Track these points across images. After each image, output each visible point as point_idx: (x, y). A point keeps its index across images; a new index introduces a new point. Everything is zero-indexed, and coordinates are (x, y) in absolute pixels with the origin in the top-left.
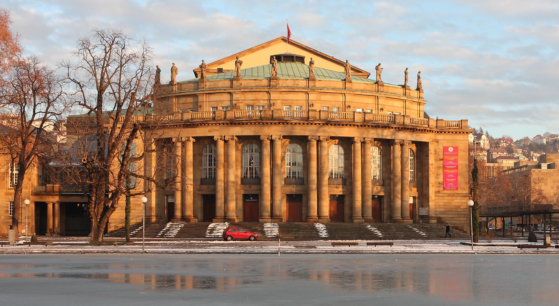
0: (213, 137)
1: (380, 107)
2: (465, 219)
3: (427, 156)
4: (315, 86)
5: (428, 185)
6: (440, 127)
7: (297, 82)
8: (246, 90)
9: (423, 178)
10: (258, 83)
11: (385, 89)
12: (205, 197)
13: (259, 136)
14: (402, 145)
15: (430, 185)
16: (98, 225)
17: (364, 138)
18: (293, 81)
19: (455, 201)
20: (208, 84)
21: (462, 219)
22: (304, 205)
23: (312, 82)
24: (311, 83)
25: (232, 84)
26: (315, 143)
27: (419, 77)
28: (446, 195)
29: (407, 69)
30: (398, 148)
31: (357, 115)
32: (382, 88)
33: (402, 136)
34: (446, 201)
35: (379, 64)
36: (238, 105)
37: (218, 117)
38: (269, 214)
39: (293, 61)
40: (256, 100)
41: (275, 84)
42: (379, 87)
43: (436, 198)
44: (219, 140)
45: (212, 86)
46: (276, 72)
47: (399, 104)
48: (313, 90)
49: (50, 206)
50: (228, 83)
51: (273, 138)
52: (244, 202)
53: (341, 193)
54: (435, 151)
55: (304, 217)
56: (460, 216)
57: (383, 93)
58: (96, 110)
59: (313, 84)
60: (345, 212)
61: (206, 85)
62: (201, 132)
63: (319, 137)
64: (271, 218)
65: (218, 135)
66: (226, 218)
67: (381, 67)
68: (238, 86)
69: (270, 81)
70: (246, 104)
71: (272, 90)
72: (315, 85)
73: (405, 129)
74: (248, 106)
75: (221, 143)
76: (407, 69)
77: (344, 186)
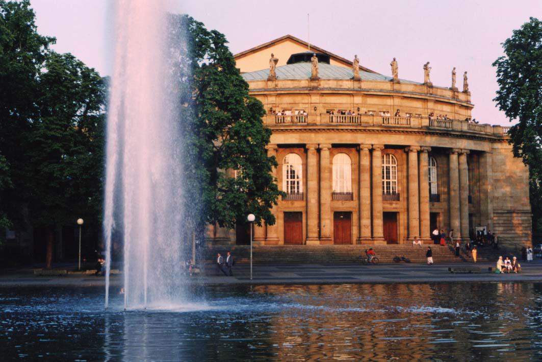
7: (340, 83)
10: (296, 84)
14: (460, 155)
18: (335, 82)
26: (368, 152)
28: (506, 212)
29: (454, 69)
30: (454, 158)
32: (431, 90)
34: (505, 218)
35: (428, 63)
38: (316, 235)
40: (295, 104)
43: (495, 215)
52: (285, 221)
57: (433, 96)
59: (359, 85)
60: (399, 230)
64: (319, 240)
66: (267, 240)
67: (429, 66)
72: (361, 86)
76: (454, 69)
77: (398, 202)
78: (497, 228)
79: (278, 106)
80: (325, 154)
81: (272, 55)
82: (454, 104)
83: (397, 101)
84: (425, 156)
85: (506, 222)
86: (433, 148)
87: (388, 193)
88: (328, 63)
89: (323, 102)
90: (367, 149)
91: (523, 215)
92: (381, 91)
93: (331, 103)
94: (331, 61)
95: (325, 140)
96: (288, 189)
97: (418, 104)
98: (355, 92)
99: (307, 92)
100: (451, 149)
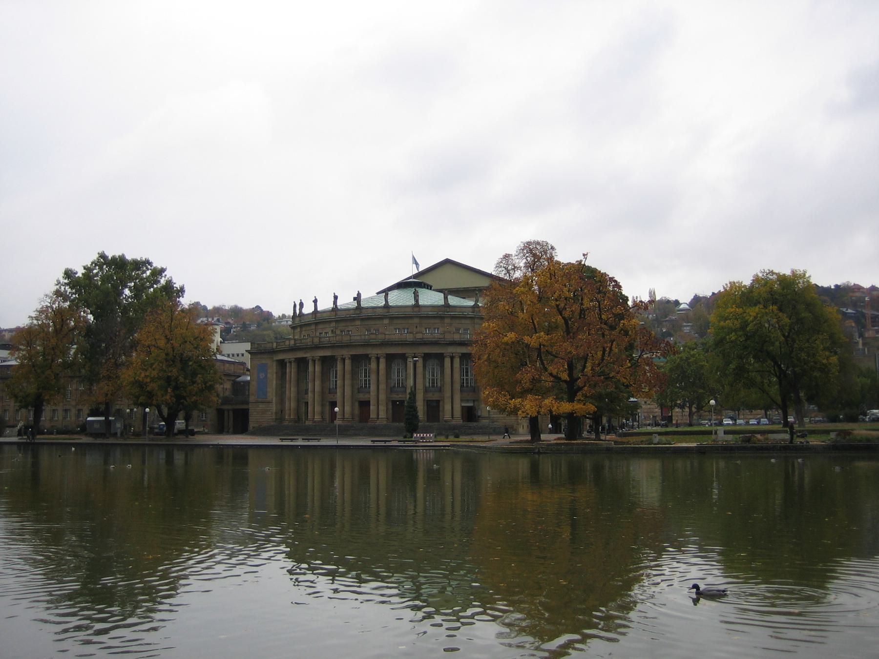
0: (306, 357)
4: (389, 311)
7: (375, 310)
13: (334, 356)
33: (450, 350)
49: (226, 413)
57: (450, 313)
80: (348, 362)
81: (334, 294)
83: (416, 321)
87: (467, 386)
89: (364, 324)
95: (346, 353)
96: (429, 384)
97: (437, 321)
100: (443, 354)
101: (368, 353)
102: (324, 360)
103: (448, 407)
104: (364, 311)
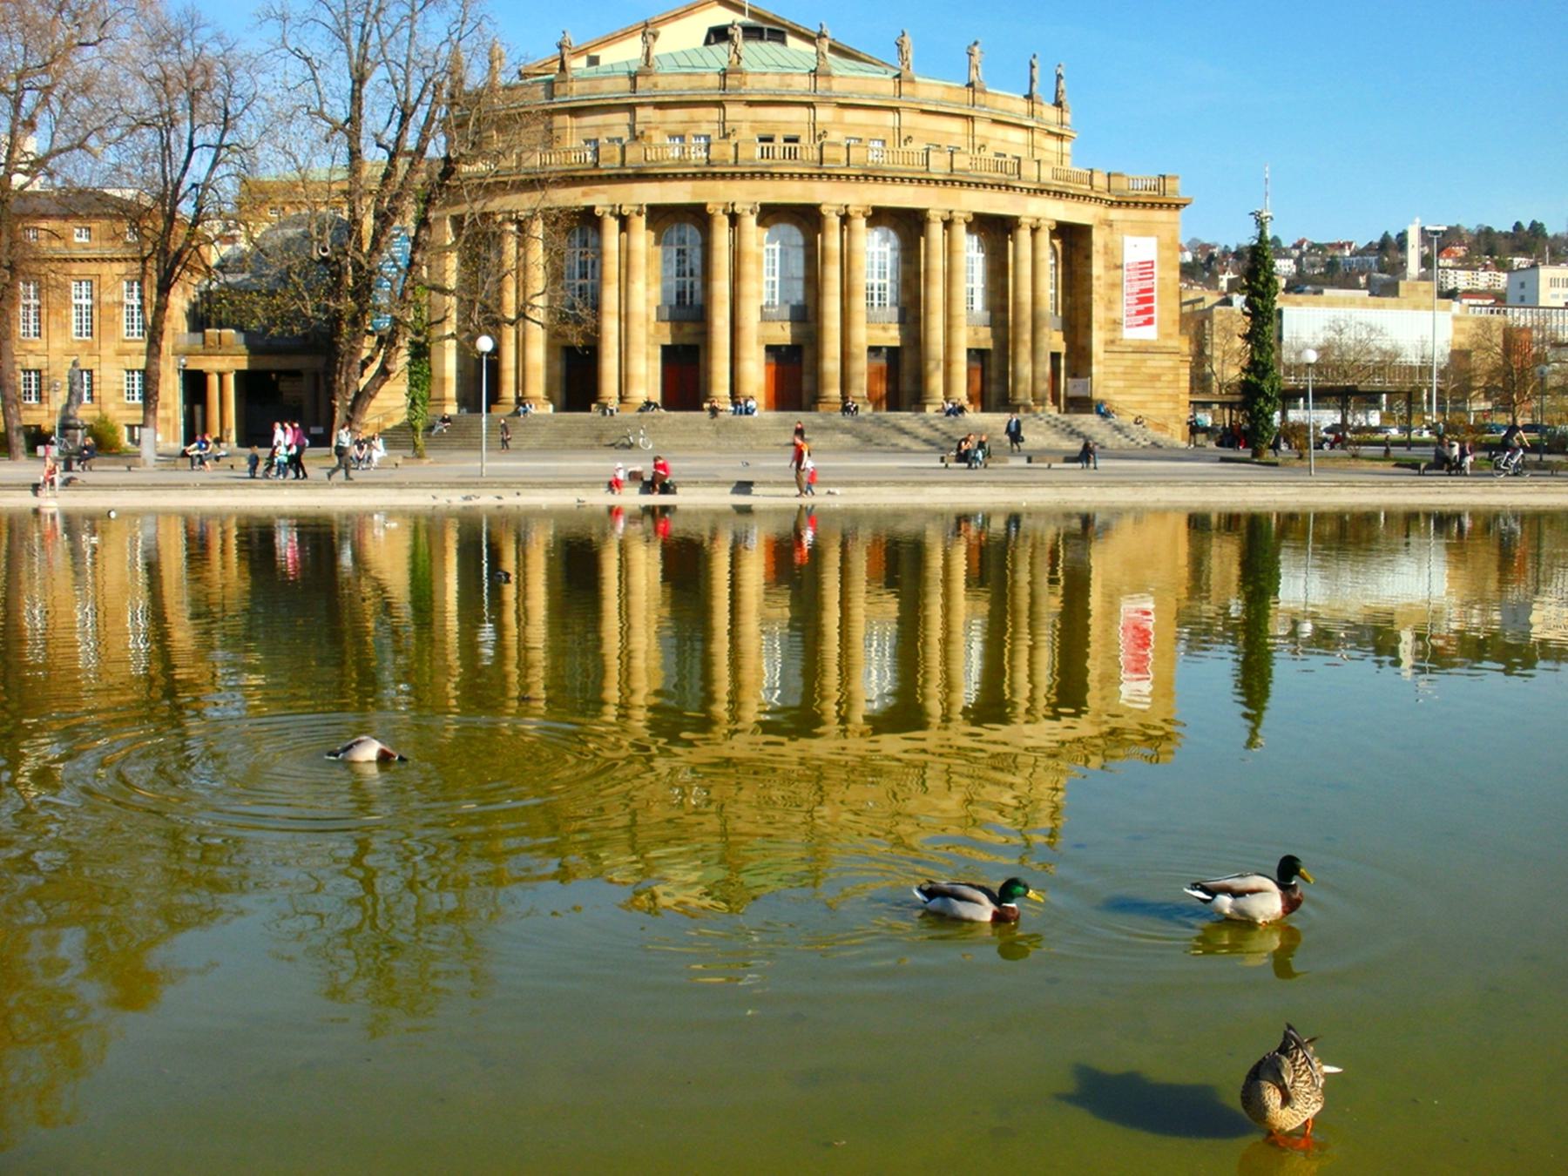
0: (593, 208)
1: (978, 142)
2: (1171, 405)
3: (1088, 257)
4: (829, 89)
5: (1089, 326)
6: (1116, 190)
7: (788, 79)
8: (667, 99)
9: (1076, 309)
10: (696, 82)
11: (988, 100)
12: (569, 351)
15: (1095, 326)
16: (348, 417)
17: (951, 212)
18: (777, 78)
19: (1150, 363)
20: (576, 86)
21: (1164, 405)
22: (805, 369)
23: (824, 79)
24: (821, 83)
25: (634, 85)
26: (837, 221)
27: (1059, 77)
29: (1034, 56)
30: (1024, 235)
31: (936, 157)
34: (1129, 363)
36: (647, 133)
37: (605, 160)
39: (761, 38)
41: (736, 83)
42: (977, 95)
44: (607, 216)
45: (587, 91)
46: (739, 58)
47: (1018, 136)
48: (826, 102)
50: (625, 84)
51: (738, 209)
53: (897, 343)
54: (1106, 246)
55: (806, 399)
56: (1160, 398)
58: (348, 126)
61: (571, 89)
62: (574, 197)
63: (847, 207)
65: (606, 203)
68: (650, 90)
69: (725, 76)
70: (666, 131)
71: (729, 98)
73: (1042, 192)
74: (672, 137)
75: (612, 226)
78: (1111, 383)
79: (657, 128)
82: (1032, 128)
83: (907, 118)
84: (960, 230)
85: (1129, 370)
86: (976, 215)
88: (783, 42)
89: (751, 118)
90: (834, 214)
91: (1166, 356)
92: (874, 96)
93: (767, 122)
94: (790, 39)
95: (747, 195)
97: (957, 126)
98: (817, 99)
99: (717, 98)
101: (818, 202)
102: (660, 216)
103: (1025, 369)
104: (749, 79)
